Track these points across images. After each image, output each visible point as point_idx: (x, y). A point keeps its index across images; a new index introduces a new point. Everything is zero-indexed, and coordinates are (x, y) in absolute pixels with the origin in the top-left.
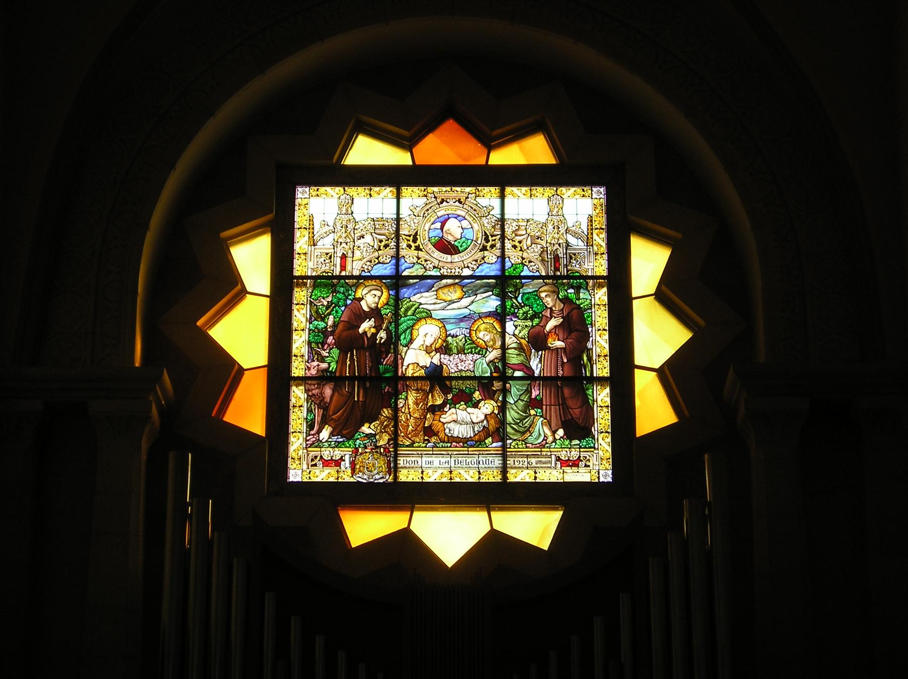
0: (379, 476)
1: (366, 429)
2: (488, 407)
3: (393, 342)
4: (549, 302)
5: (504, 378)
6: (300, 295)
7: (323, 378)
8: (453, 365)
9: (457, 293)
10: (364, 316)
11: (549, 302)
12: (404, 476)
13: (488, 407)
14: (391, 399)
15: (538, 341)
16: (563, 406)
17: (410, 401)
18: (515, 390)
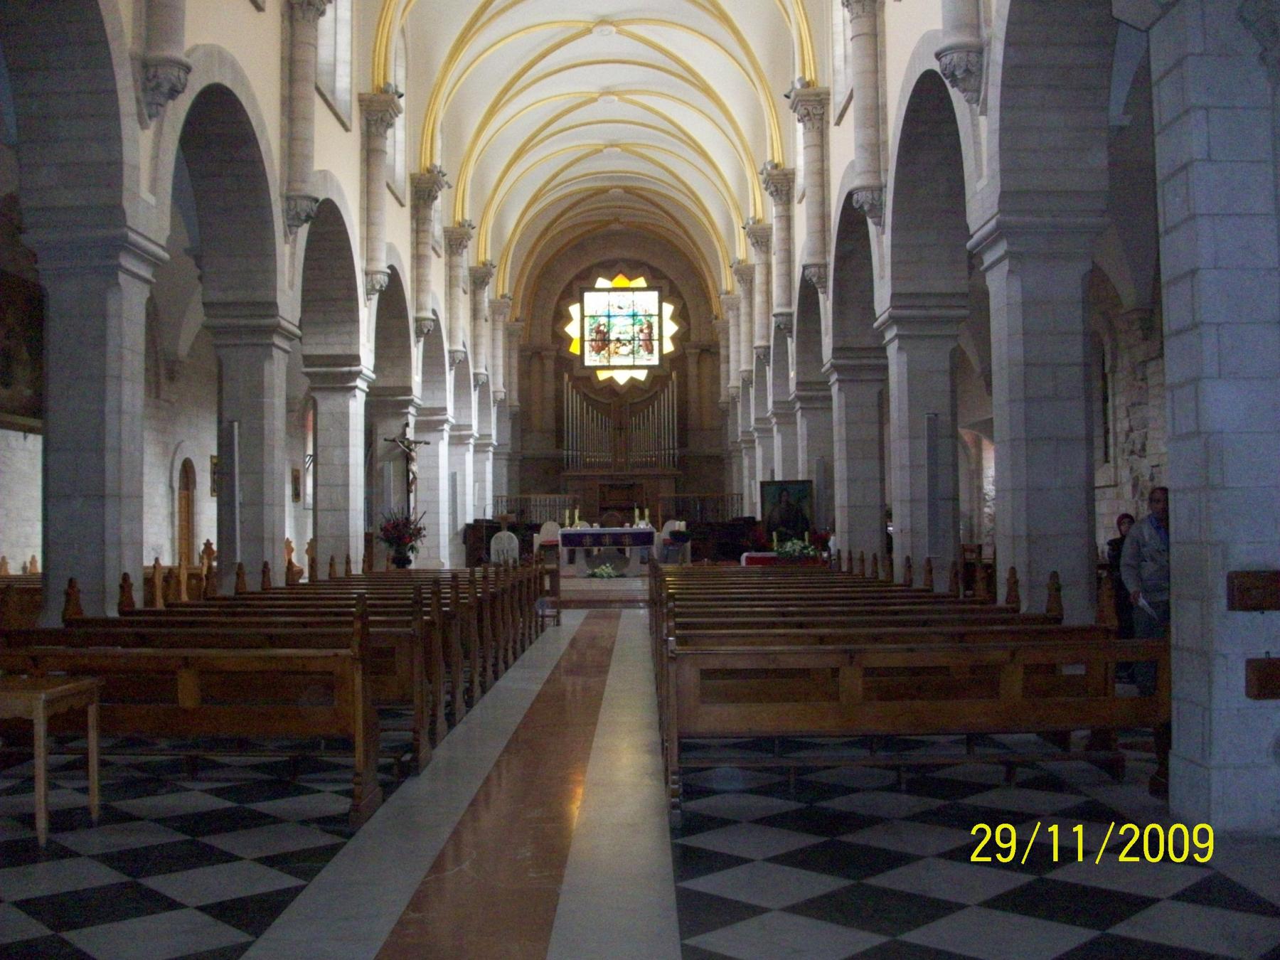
0: (606, 364)
1: (603, 352)
2: (631, 347)
3: (608, 332)
4: (644, 321)
5: (633, 340)
6: (587, 320)
7: (592, 340)
8: (622, 337)
9: (622, 319)
10: (600, 325)
11: (644, 321)
12: (612, 364)
13: (631, 347)
14: (607, 345)
15: (641, 331)
16: (647, 345)
17: (612, 346)
18: (636, 342)
